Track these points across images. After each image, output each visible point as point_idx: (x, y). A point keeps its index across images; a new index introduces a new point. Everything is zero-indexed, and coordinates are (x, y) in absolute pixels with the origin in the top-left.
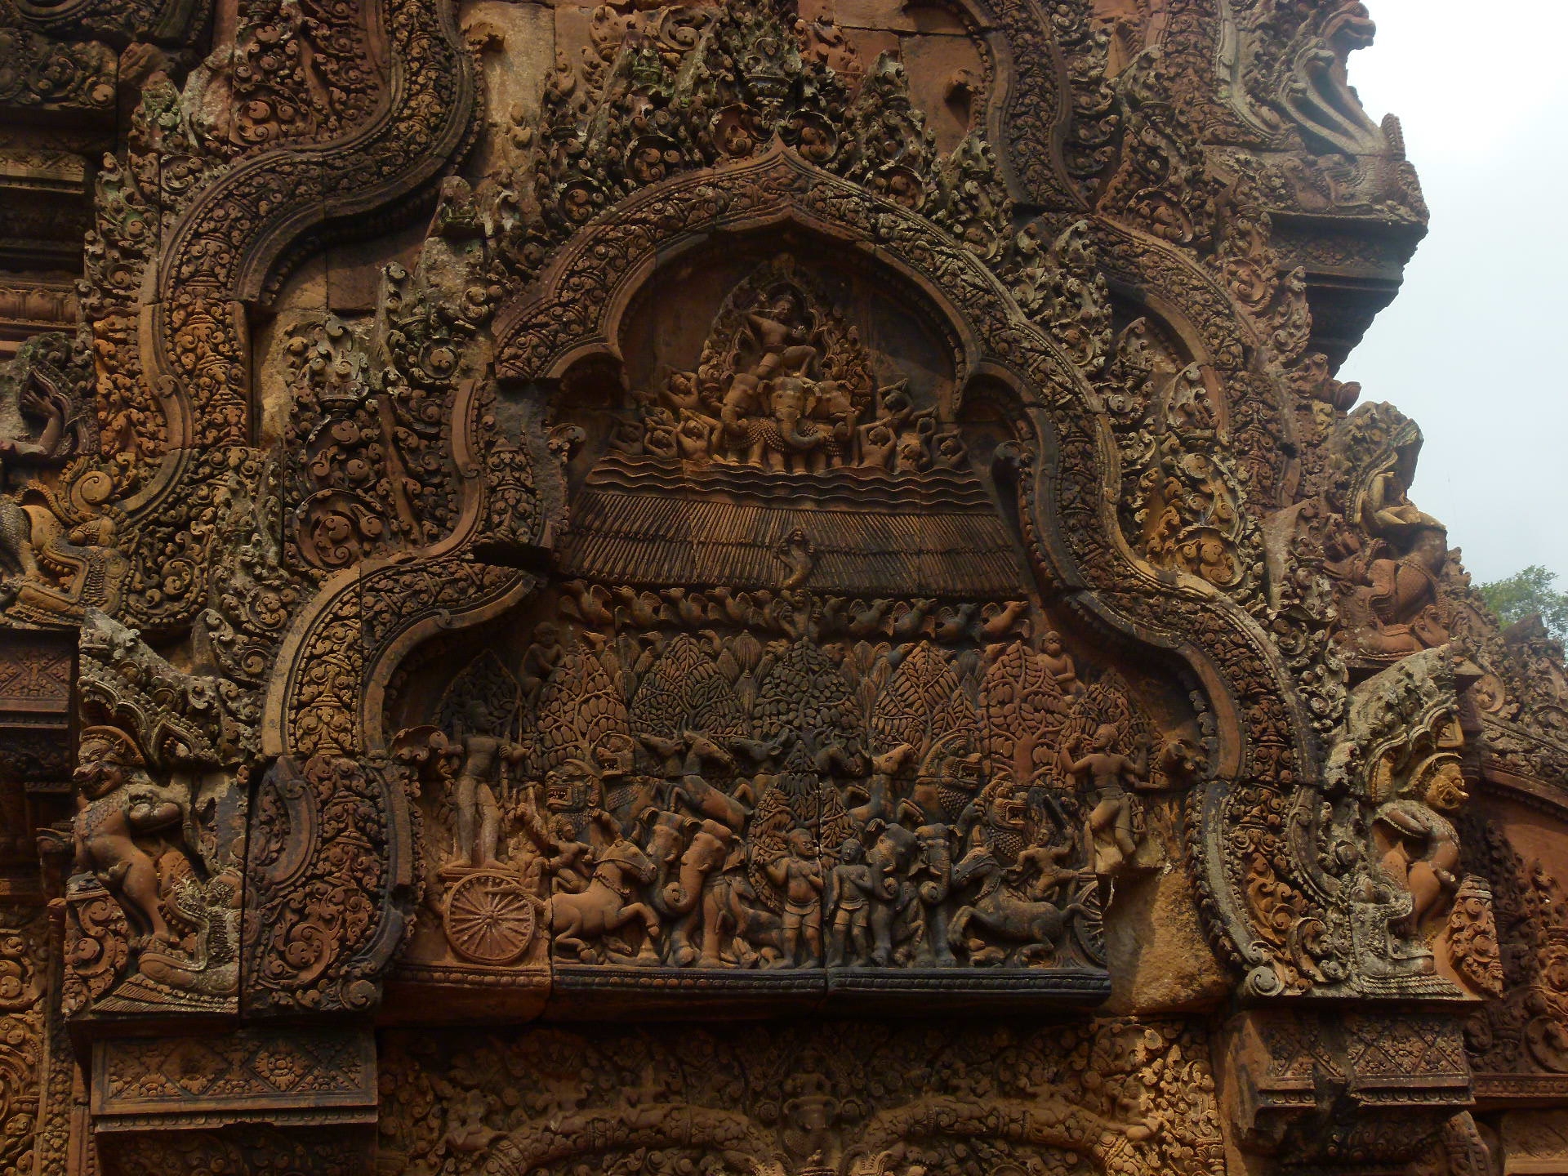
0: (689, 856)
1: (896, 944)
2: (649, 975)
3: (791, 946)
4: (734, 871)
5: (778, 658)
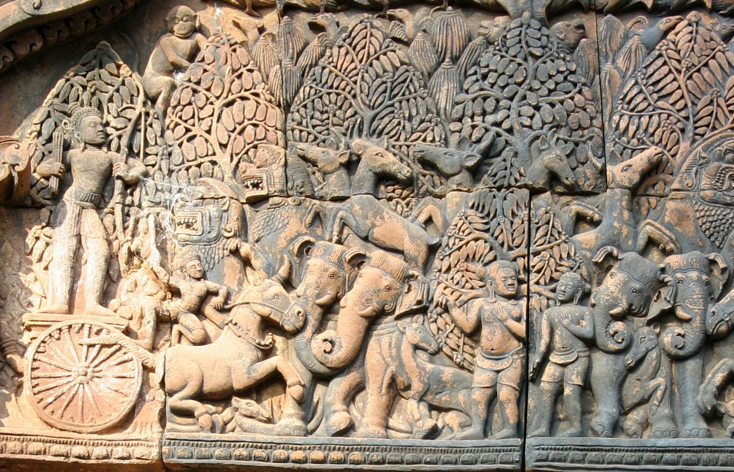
0: (349, 300)
1: (624, 411)
2: (285, 446)
3: (480, 410)
4: (410, 313)
5: (489, 43)
